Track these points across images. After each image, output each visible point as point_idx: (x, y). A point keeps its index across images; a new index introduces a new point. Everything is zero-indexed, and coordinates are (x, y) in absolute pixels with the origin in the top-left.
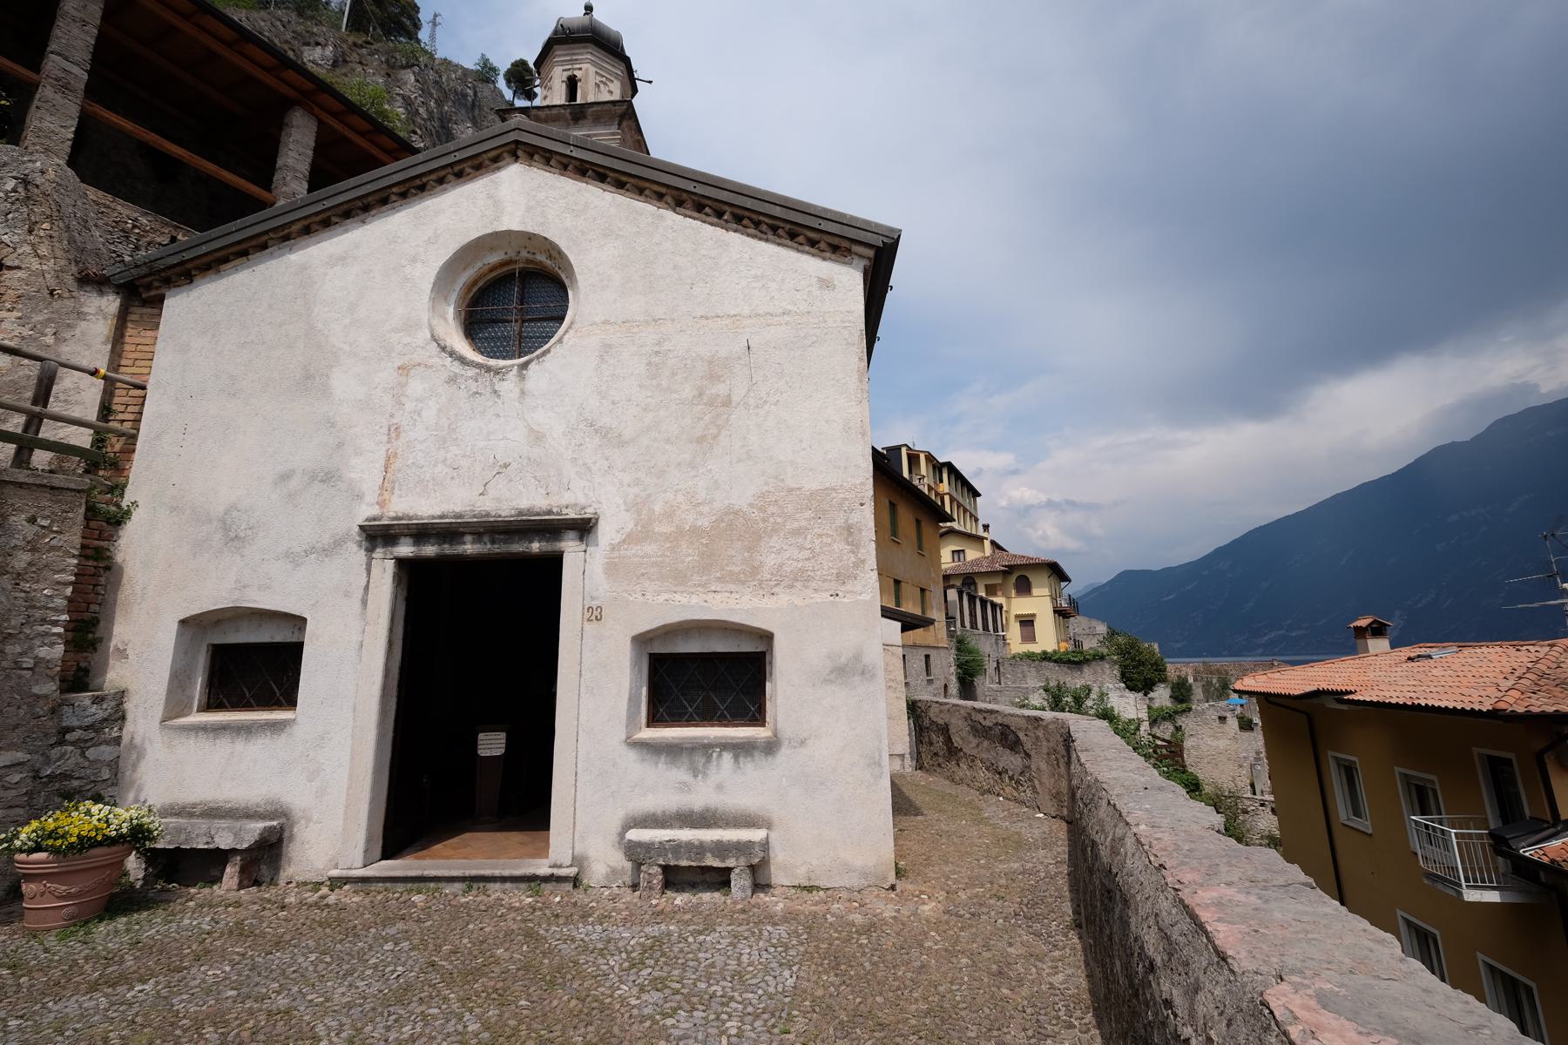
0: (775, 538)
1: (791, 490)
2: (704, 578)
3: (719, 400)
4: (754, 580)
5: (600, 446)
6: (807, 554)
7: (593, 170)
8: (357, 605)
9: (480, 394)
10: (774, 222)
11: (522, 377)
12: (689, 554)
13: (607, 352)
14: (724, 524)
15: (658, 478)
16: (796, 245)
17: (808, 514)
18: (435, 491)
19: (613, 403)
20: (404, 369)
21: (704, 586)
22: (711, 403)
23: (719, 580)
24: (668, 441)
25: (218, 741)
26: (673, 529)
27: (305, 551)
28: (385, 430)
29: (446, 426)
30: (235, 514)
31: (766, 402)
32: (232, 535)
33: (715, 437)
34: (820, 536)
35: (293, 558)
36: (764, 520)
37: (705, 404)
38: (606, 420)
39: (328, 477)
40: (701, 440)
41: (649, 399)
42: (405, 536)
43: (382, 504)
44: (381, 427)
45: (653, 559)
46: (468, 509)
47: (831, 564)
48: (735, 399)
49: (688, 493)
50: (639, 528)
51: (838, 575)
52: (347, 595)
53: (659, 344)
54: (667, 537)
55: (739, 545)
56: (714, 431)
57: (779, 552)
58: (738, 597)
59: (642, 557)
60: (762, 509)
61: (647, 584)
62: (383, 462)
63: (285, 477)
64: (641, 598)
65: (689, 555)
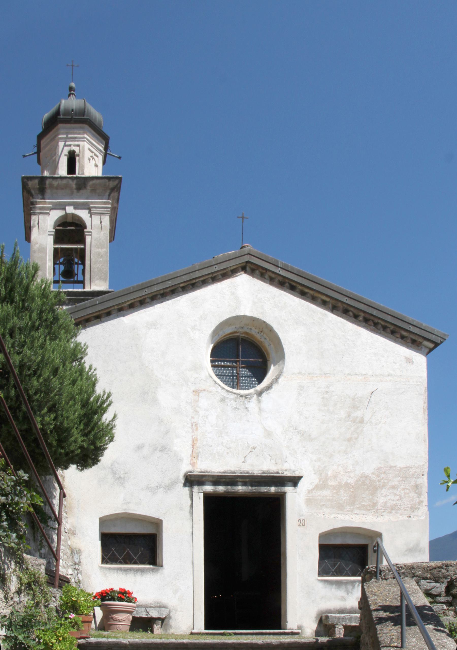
0: (384, 490)
1: (391, 467)
2: (352, 508)
3: (358, 420)
4: (374, 509)
6: (398, 497)
8: (187, 514)
9: (238, 409)
10: (386, 324)
11: (259, 401)
12: (344, 496)
13: (301, 390)
16: (394, 338)
17: (399, 479)
18: (219, 459)
19: (306, 418)
20: (196, 392)
21: (352, 511)
22: (354, 421)
23: (358, 508)
24: (334, 439)
26: (337, 483)
27: (157, 487)
30: (117, 465)
31: (380, 422)
32: (118, 476)
33: (356, 439)
34: (404, 489)
35: (153, 490)
36: (379, 481)
37: (351, 421)
39: (163, 449)
40: (350, 440)
42: (208, 481)
43: (193, 464)
44: (188, 424)
45: (328, 498)
46: (237, 469)
47: (408, 503)
48: (366, 419)
49: (344, 466)
50: (321, 483)
51: (411, 508)
52: (181, 509)
53: (327, 387)
54: (334, 487)
55: (367, 492)
56: (356, 435)
57: (386, 496)
58: (366, 516)
59: (323, 497)
60: (378, 476)
61: (325, 509)
62: (190, 442)
63: (140, 447)
64: (323, 516)
65: (344, 496)
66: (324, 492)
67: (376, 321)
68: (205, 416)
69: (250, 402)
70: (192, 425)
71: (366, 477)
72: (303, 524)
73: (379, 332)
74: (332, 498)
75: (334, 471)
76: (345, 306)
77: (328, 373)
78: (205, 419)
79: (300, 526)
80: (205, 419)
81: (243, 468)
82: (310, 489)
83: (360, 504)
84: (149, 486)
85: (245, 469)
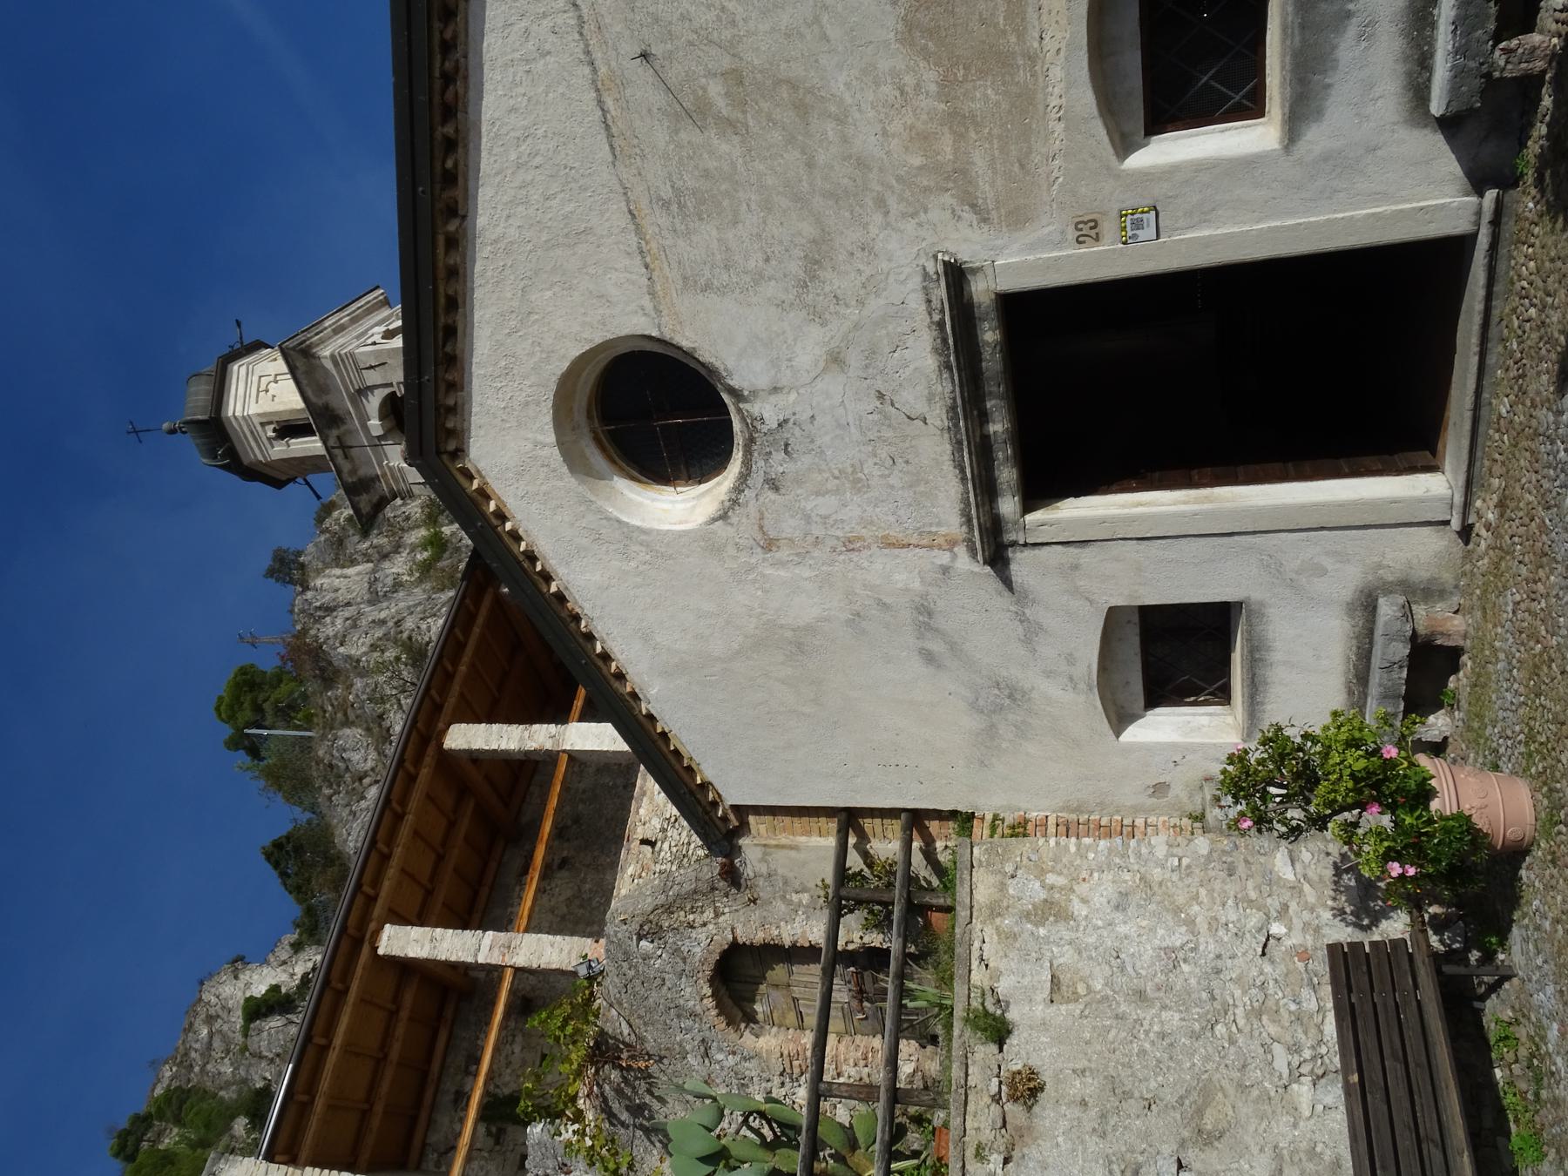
5: (834, 268)
7: (444, 346)
9: (787, 445)
10: (437, 49)
11: (754, 393)
12: (985, 96)
14: (930, 44)
15: (870, 170)
19: (767, 260)
21: (1032, 58)
23: (1021, 35)
24: (810, 165)
25: (1269, 680)
26: (946, 129)
27: (1021, 621)
28: (854, 555)
29: (837, 481)
30: (981, 702)
32: (1007, 701)
35: (1031, 633)
37: (744, 112)
38: (795, 268)
39: (924, 611)
40: (802, 109)
41: (753, 207)
42: (992, 508)
46: (946, 436)
48: (726, 62)
50: (951, 185)
53: (666, 205)
54: (960, 137)
56: (784, 92)
59: (995, 172)
63: (929, 657)
65: (986, 95)
66: (980, 172)
67: (438, 84)
68: (825, 523)
69: (762, 419)
70: (853, 550)
71: (910, 25)
72: (1091, 228)
73: (462, 60)
74: (995, 141)
75: (907, 149)
76: (438, 187)
77: (626, 210)
78: (831, 521)
79: (1097, 234)
80: (831, 521)
81: (942, 420)
82: (974, 218)
83: (1004, 32)
84: (1023, 638)
85: (944, 417)
